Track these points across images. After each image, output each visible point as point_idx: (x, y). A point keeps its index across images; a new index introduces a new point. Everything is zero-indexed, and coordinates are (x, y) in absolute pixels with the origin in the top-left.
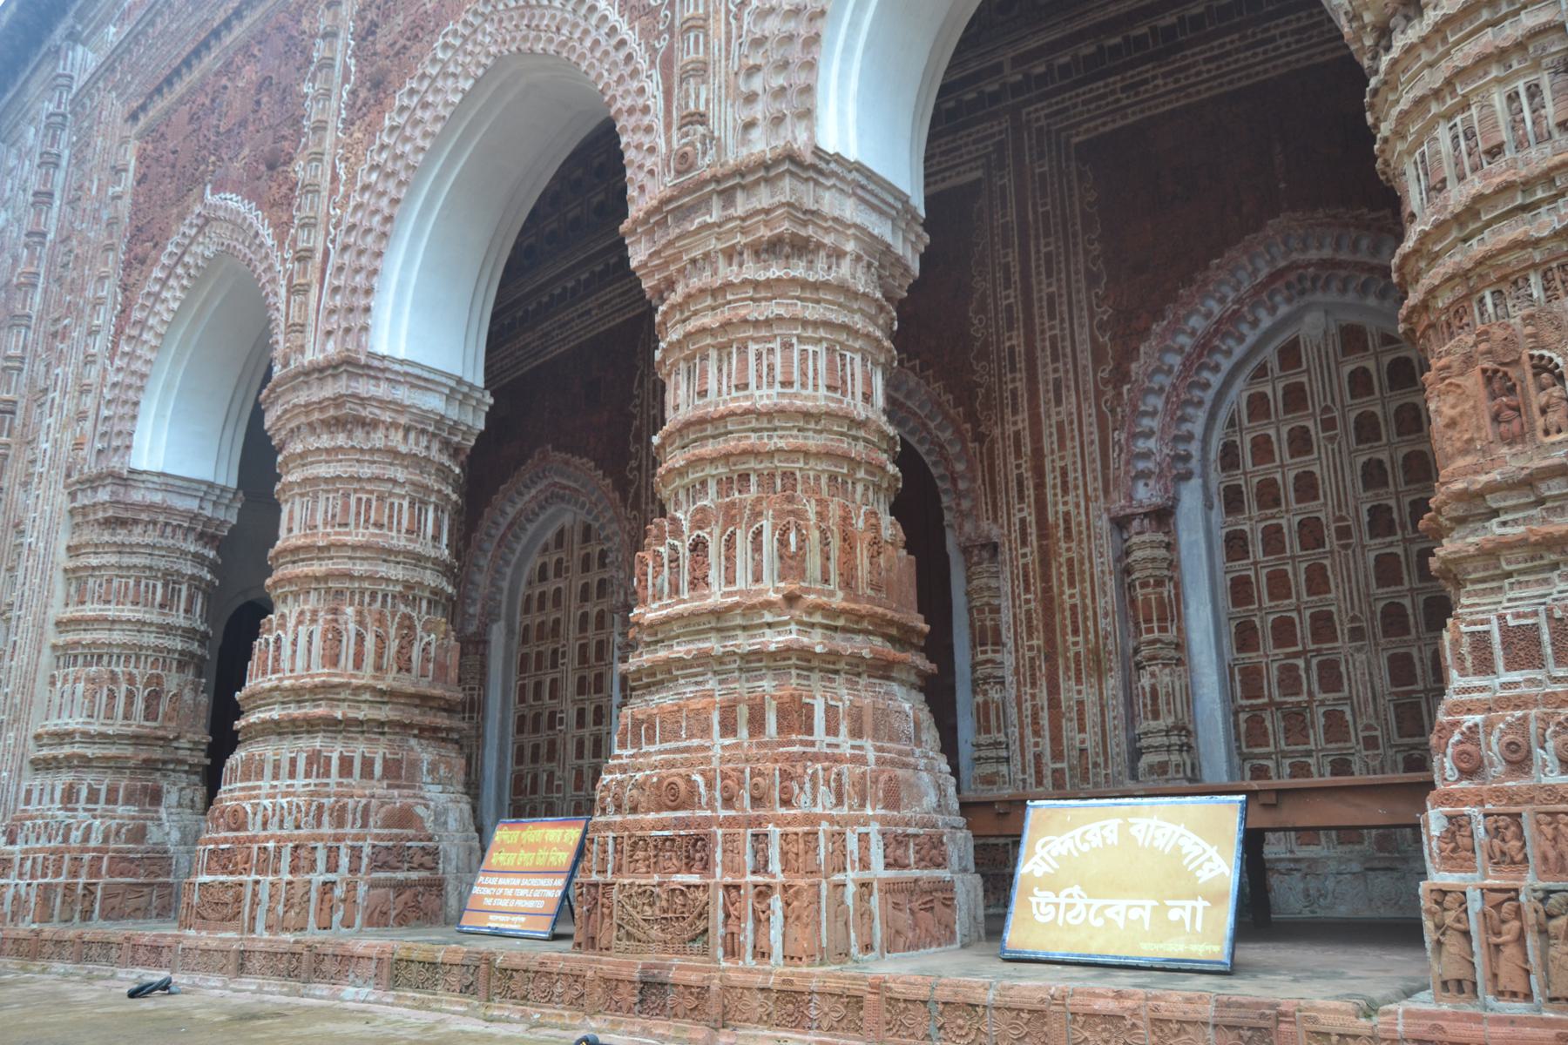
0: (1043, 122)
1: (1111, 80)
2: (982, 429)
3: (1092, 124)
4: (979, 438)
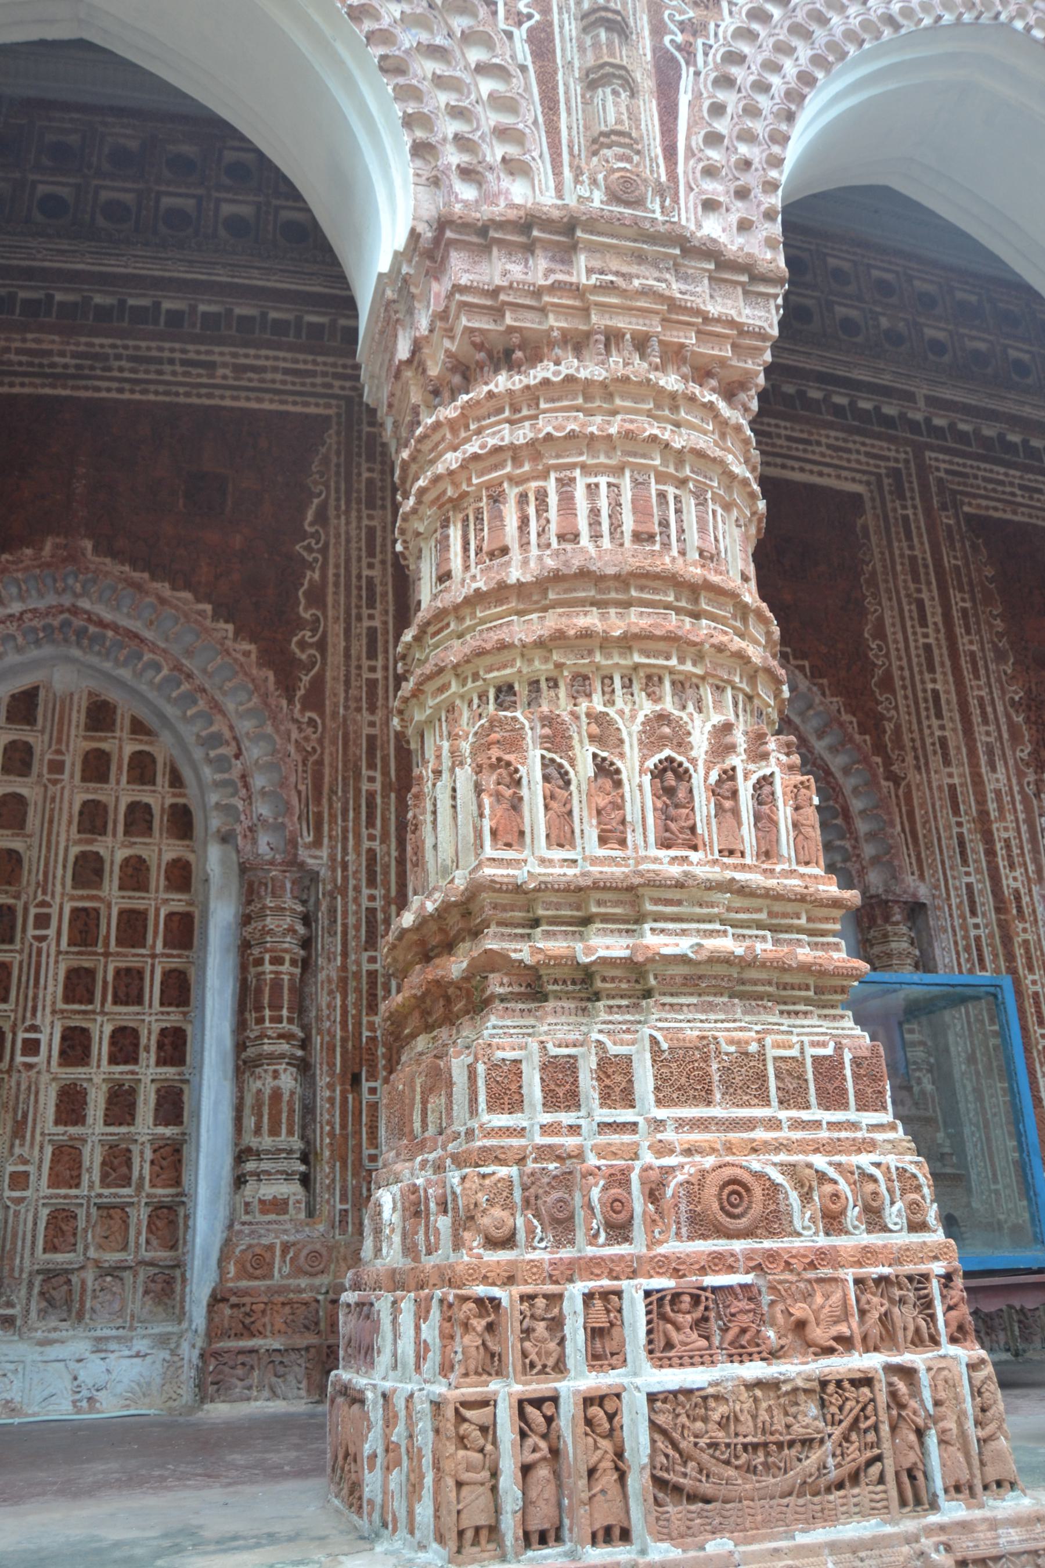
0: (942, 474)
1: (1012, 472)
2: (895, 768)
3: (984, 503)
4: (895, 779)
